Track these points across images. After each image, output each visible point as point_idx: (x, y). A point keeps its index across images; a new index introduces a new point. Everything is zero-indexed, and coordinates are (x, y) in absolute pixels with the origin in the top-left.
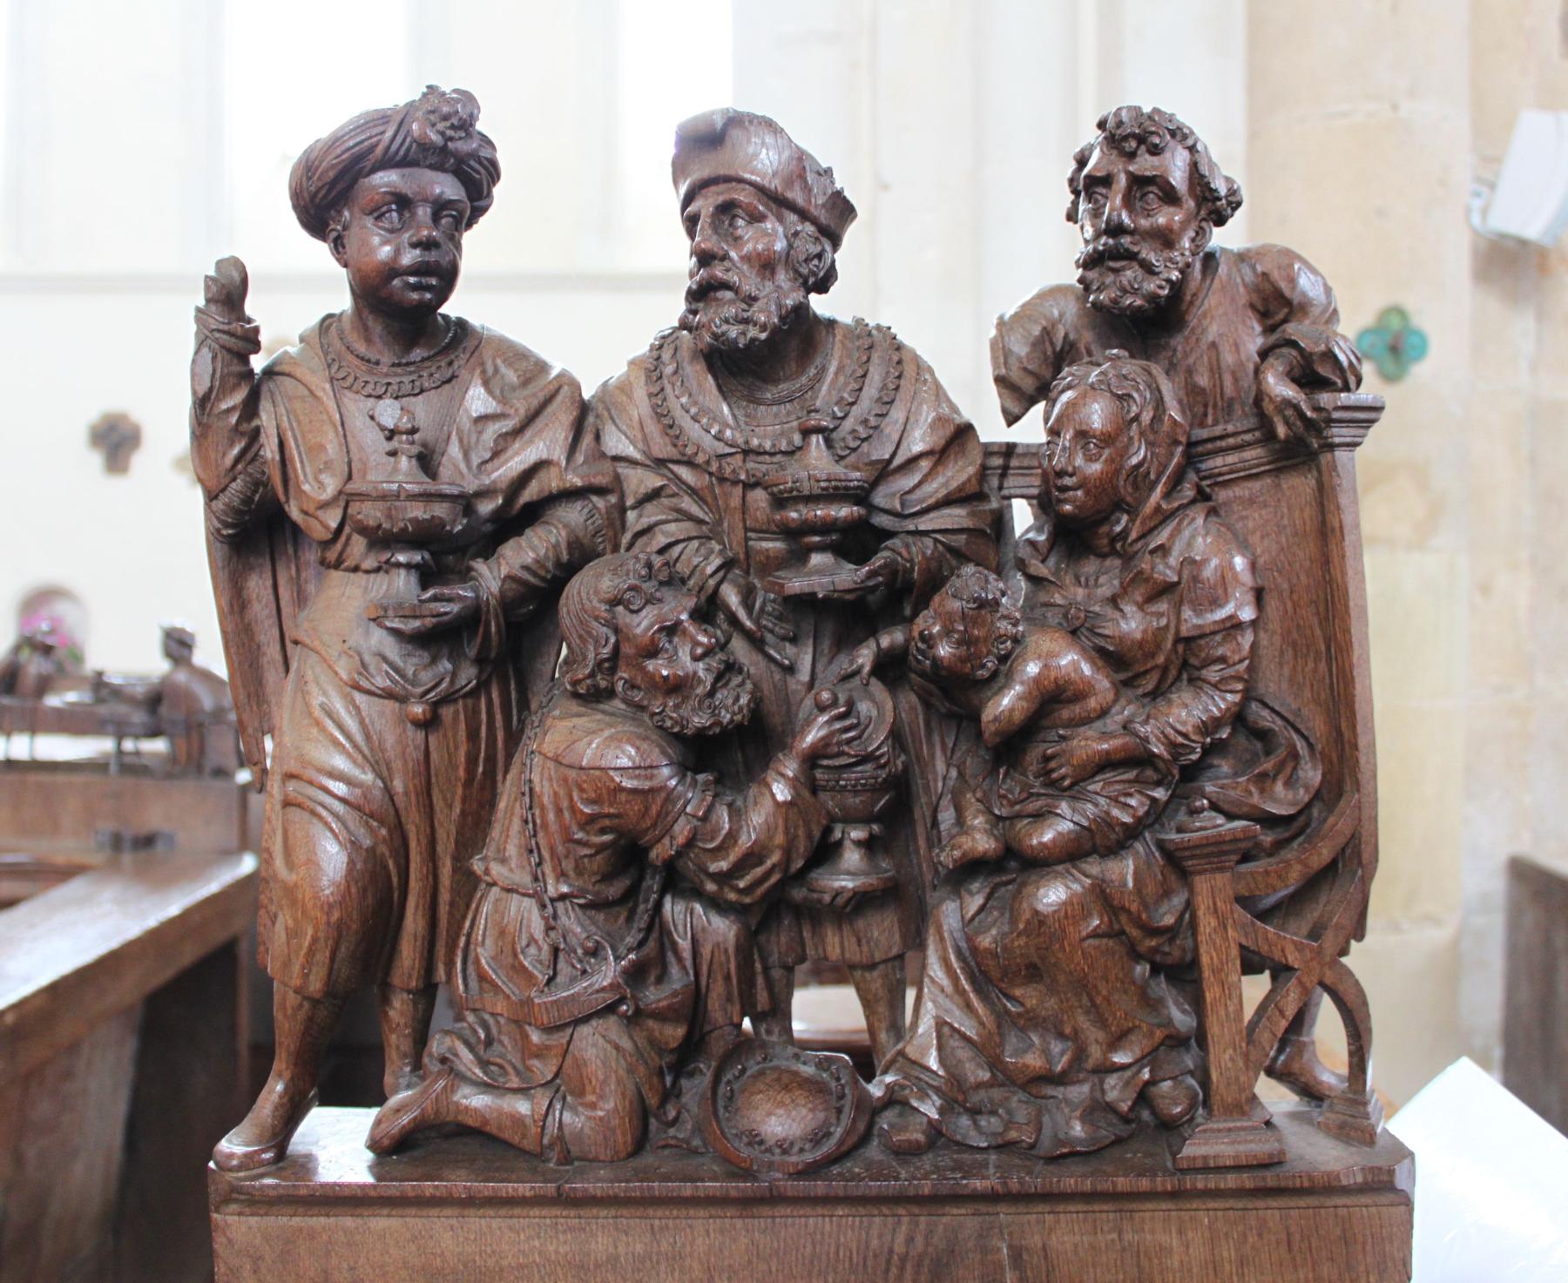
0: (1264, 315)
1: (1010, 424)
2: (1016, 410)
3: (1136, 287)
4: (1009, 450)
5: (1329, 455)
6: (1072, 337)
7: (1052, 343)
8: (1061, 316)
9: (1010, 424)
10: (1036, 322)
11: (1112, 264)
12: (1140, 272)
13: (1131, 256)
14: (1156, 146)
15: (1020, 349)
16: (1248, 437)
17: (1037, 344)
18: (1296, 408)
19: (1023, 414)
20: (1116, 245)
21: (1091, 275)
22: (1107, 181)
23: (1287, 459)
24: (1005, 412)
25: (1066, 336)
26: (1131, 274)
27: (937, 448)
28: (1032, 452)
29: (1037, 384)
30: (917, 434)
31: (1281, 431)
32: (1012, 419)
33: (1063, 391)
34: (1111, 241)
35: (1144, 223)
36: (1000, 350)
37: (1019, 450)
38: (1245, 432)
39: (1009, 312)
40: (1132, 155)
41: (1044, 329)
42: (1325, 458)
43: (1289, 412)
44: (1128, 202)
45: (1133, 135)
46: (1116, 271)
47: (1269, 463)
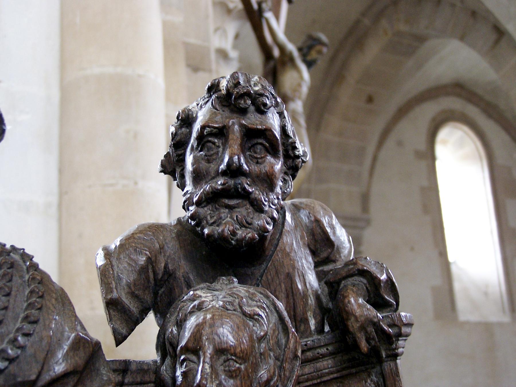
0: (314, 253)
1: (118, 343)
2: (124, 331)
3: (226, 224)
4: (124, 367)
5: (392, 364)
6: (170, 267)
7: (155, 273)
8: (162, 248)
9: (118, 343)
10: (141, 253)
11: (226, 201)
12: (251, 209)
13: (246, 195)
14: (265, 105)
15: (126, 275)
16: (323, 350)
17: (143, 270)
18: (376, 325)
19: (129, 334)
20: (235, 186)
21: (206, 211)
22: (222, 133)
23: (353, 367)
24: (115, 332)
25: (166, 267)
26: (244, 211)
27: (80, 369)
28: (143, 368)
29: (141, 308)
30: (60, 355)
31: (364, 346)
32: (119, 339)
33: (192, 313)
34: (231, 182)
35: (255, 168)
36: (105, 275)
37: (133, 367)
38: (320, 347)
39: (114, 244)
40: (243, 112)
41: (149, 259)
42: (387, 366)
43: (371, 329)
44: (243, 149)
45: (248, 94)
46: (231, 208)
47: (338, 371)
